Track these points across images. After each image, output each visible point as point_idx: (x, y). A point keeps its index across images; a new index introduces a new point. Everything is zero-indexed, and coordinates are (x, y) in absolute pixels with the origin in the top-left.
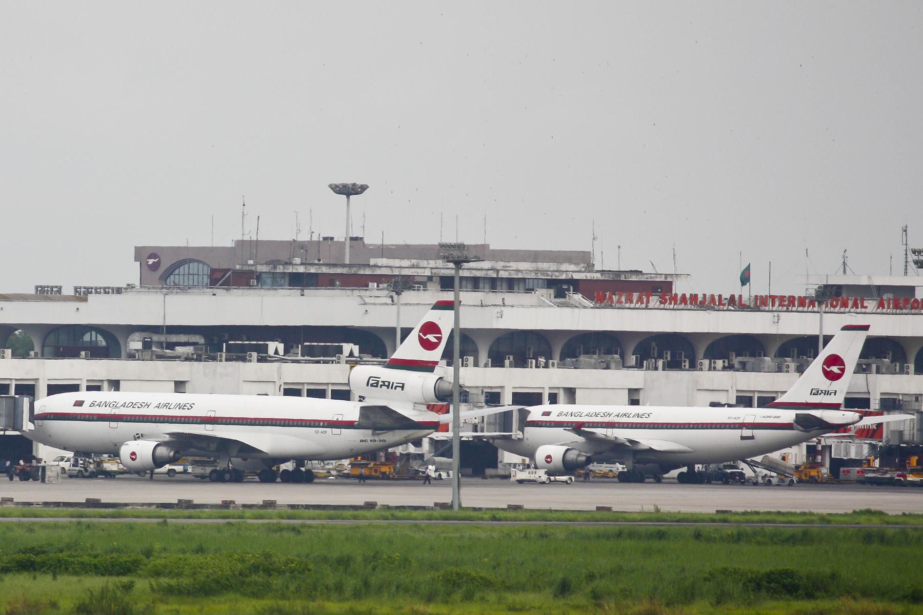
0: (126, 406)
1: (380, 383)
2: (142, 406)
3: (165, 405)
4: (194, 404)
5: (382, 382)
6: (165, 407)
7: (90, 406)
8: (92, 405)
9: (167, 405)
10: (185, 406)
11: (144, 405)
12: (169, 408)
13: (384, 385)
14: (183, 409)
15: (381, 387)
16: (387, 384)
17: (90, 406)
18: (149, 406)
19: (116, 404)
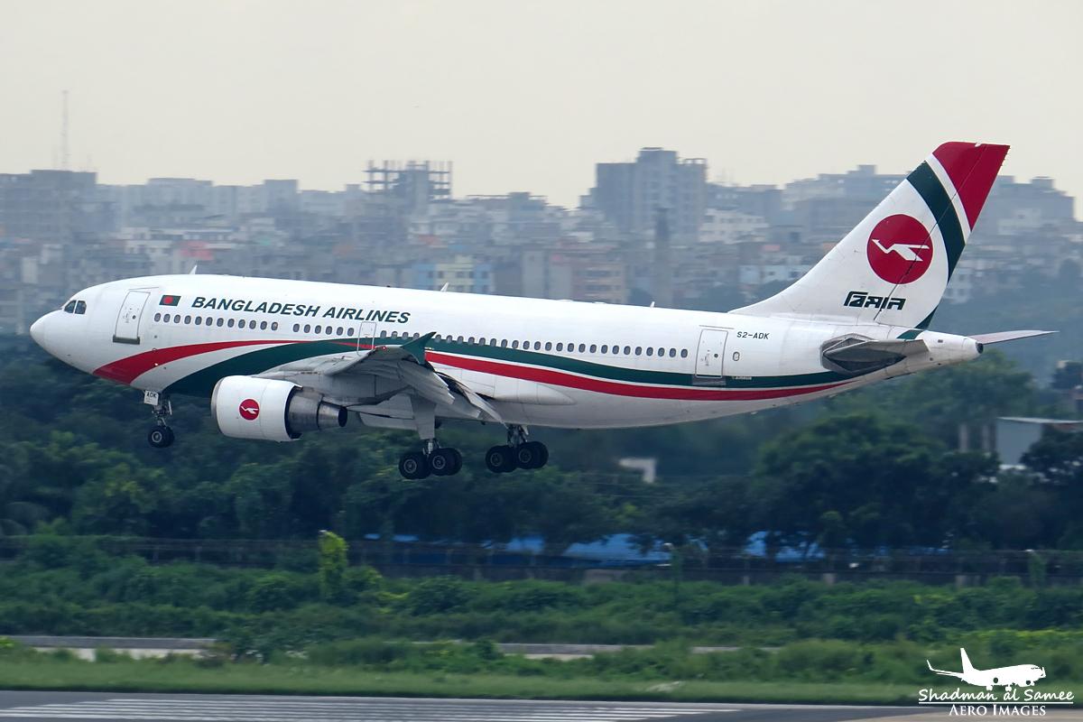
1: (867, 300)
2: (302, 312)
3: (346, 313)
4: (409, 314)
5: (869, 298)
6: (348, 316)
8: (198, 304)
9: (350, 312)
10: (390, 316)
11: (305, 310)
13: (872, 302)
14: (387, 320)
15: (866, 306)
16: (876, 300)
18: (316, 311)
19: (245, 305)
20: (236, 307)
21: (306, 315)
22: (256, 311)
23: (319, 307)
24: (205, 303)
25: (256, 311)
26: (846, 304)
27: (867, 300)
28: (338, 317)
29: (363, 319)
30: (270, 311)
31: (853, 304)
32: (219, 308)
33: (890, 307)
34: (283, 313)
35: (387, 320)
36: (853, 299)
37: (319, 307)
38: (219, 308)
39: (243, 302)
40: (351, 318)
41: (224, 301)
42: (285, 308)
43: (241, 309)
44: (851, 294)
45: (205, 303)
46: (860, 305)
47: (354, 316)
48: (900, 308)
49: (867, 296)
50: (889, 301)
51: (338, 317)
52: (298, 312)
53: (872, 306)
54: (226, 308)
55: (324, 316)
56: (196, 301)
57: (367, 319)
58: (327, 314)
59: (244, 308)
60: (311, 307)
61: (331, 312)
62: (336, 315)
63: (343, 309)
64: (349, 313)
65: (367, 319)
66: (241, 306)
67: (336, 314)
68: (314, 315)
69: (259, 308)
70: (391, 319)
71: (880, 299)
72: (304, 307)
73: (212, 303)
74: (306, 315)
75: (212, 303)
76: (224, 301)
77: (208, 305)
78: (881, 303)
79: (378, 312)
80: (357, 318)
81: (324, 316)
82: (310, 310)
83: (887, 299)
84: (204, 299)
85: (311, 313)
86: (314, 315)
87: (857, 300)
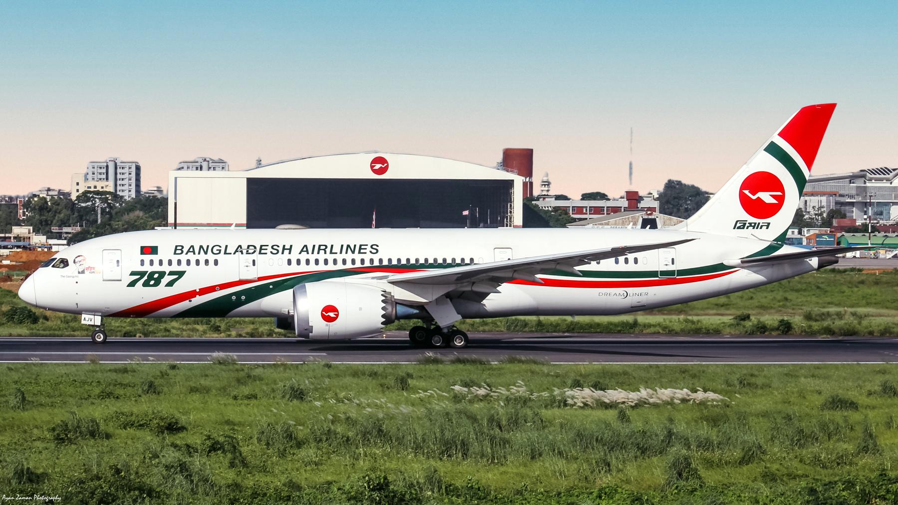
0: (244, 252)
3: (319, 249)
4: (377, 246)
6: (322, 252)
7: (175, 253)
8: (178, 252)
9: (324, 247)
10: (360, 248)
11: (280, 249)
12: (331, 253)
13: (751, 226)
14: (360, 253)
15: (747, 228)
16: (753, 225)
17: (175, 253)
18: (290, 249)
20: (215, 251)
21: (283, 253)
22: (234, 253)
23: (291, 246)
24: (185, 250)
25: (234, 253)
26: (734, 228)
27: (747, 225)
28: (313, 253)
29: (336, 253)
30: (248, 253)
31: (739, 228)
32: (199, 253)
33: (761, 228)
34: (260, 253)
35: (360, 253)
36: (738, 225)
37: (291, 246)
38: (199, 253)
39: (220, 247)
40: (325, 253)
41: (201, 247)
42: (261, 249)
43: (220, 253)
44: (737, 221)
45: (185, 250)
46: (743, 228)
47: (328, 250)
48: (767, 228)
49: (747, 222)
50: (761, 224)
51: (313, 253)
52: (276, 252)
53: (751, 228)
54: (206, 253)
55: (300, 253)
56: (176, 249)
57: (341, 253)
58: (302, 251)
59: (223, 251)
60: (284, 246)
61: (305, 249)
62: (310, 250)
63: (314, 246)
64: (322, 248)
65: (341, 253)
66: (220, 250)
67: (310, 250)
68: (290, 253)
69: (236, 251)
70: (362, 251)
71: (755, 223)
72: (278, 246)
73: (192, 249)
74: (283, 253)
75: (192, 249)
76: (201, 247)
77: (189, 251)
78: (754, 226)
79: (348, 246)
80: (331, 253)
81: (300, 253)
82: (284, 249)
83: (759, 223)
84: (183, 247)
85: (286, 252)
86: (290, 253)
87: (741, 225)
